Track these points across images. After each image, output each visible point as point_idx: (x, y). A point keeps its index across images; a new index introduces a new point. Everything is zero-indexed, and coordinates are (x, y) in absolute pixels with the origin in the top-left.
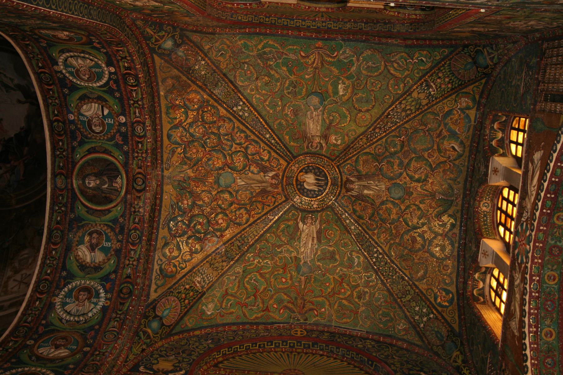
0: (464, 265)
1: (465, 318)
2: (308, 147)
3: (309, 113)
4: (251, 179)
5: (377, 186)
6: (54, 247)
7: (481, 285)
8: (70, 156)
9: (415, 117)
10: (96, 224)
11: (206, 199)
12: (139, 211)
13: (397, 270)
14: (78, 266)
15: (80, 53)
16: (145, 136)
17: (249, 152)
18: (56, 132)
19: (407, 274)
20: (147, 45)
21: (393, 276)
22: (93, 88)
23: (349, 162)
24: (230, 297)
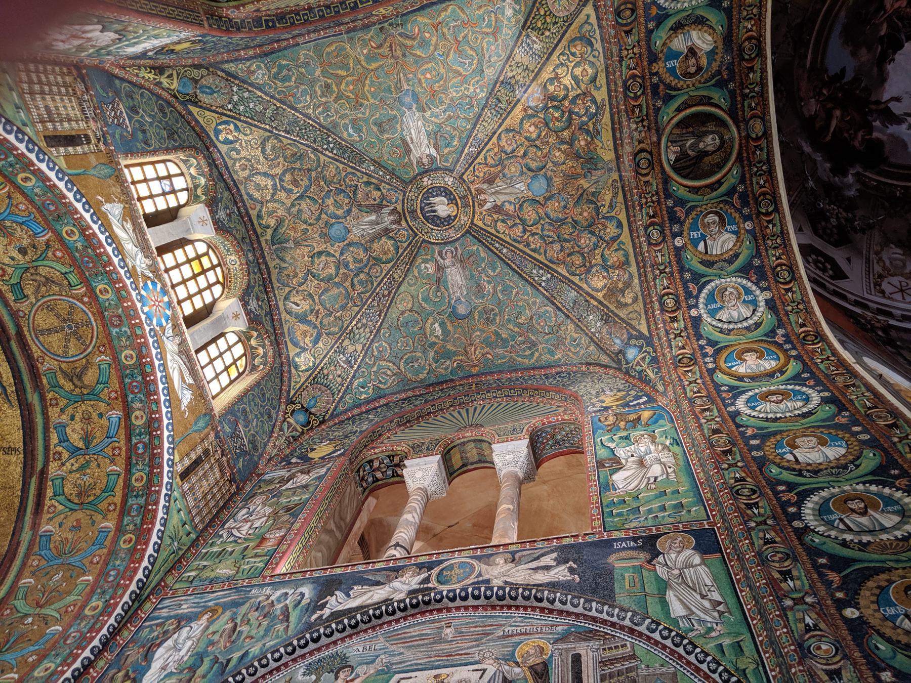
0: (224, 180)
2: (456, 249)
3: (465, 293)
4: (510, 193)
5: (363, 229)
6: (751, 33)
7: (193, 171)
8: (746, 168)
9: (351, 322)
10: (693, 85)
11: (557, 154)
12: (637, 123)
13: (298, 139)
14: (707, 20)
15: (734, 329)
16: (646, 228)
17: (520, 227)
18: (768, 197)
19: (284, 140)
20: (655, 351)
21: (300, 129)
22: (720, 276)
23: (405, 245)
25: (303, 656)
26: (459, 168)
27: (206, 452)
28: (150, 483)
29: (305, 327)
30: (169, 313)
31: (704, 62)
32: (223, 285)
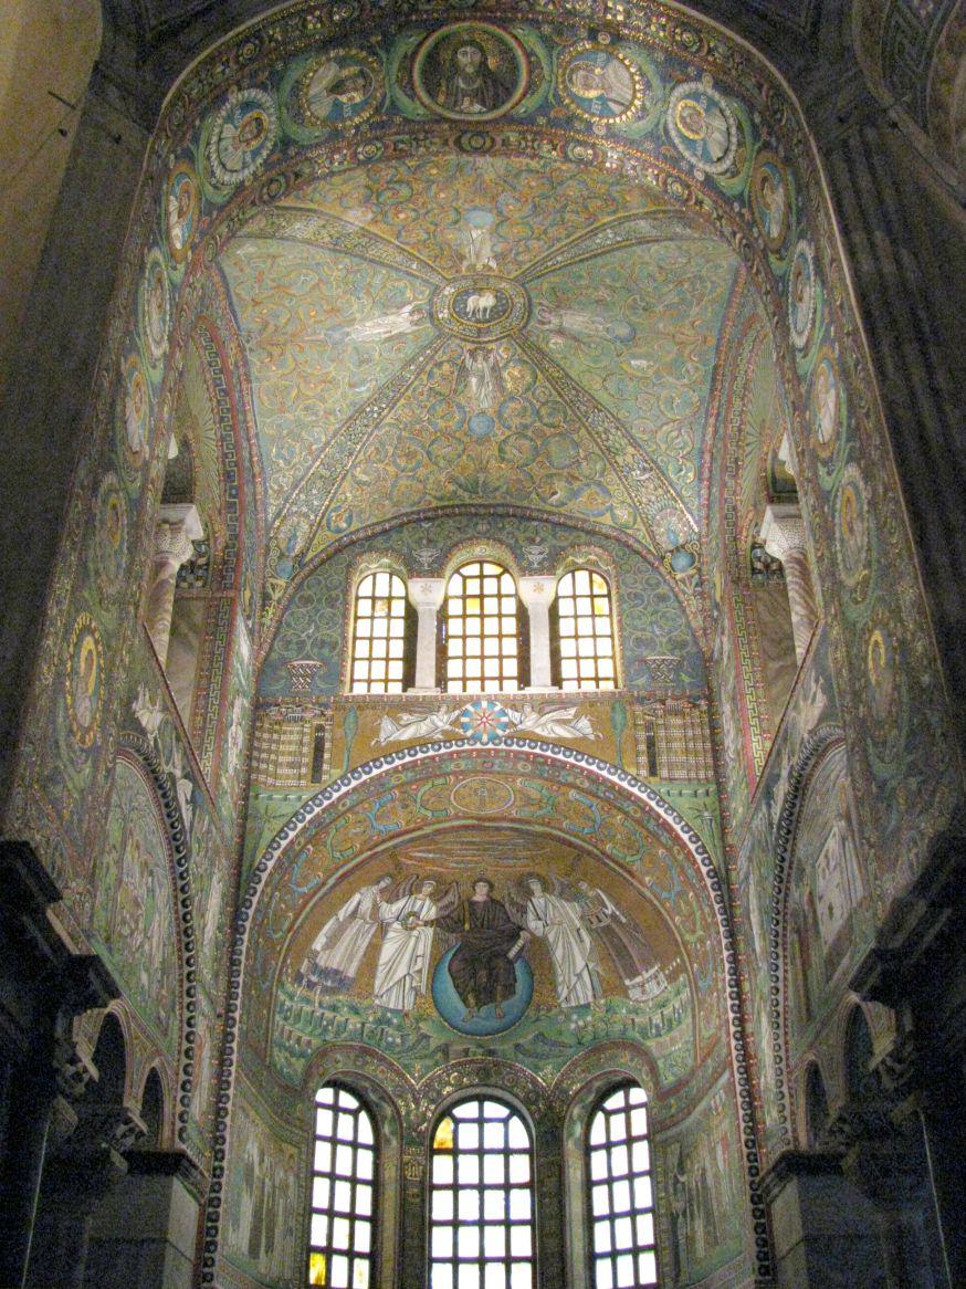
1: (323, 562)
2: (541, 304)
7: (373, 566)
9: (597, 444)
12: (418, 146)
16: (566, 159)
22: (665, 112)
23: (520, 351)
24: (269, 262)
25: (789, 875)
26: (436, 280)
27: (649, 727)
28: (643, 809)
29: (586, 494)
30: (498, 707)
31: (354, 69)
32: (506, 571)
